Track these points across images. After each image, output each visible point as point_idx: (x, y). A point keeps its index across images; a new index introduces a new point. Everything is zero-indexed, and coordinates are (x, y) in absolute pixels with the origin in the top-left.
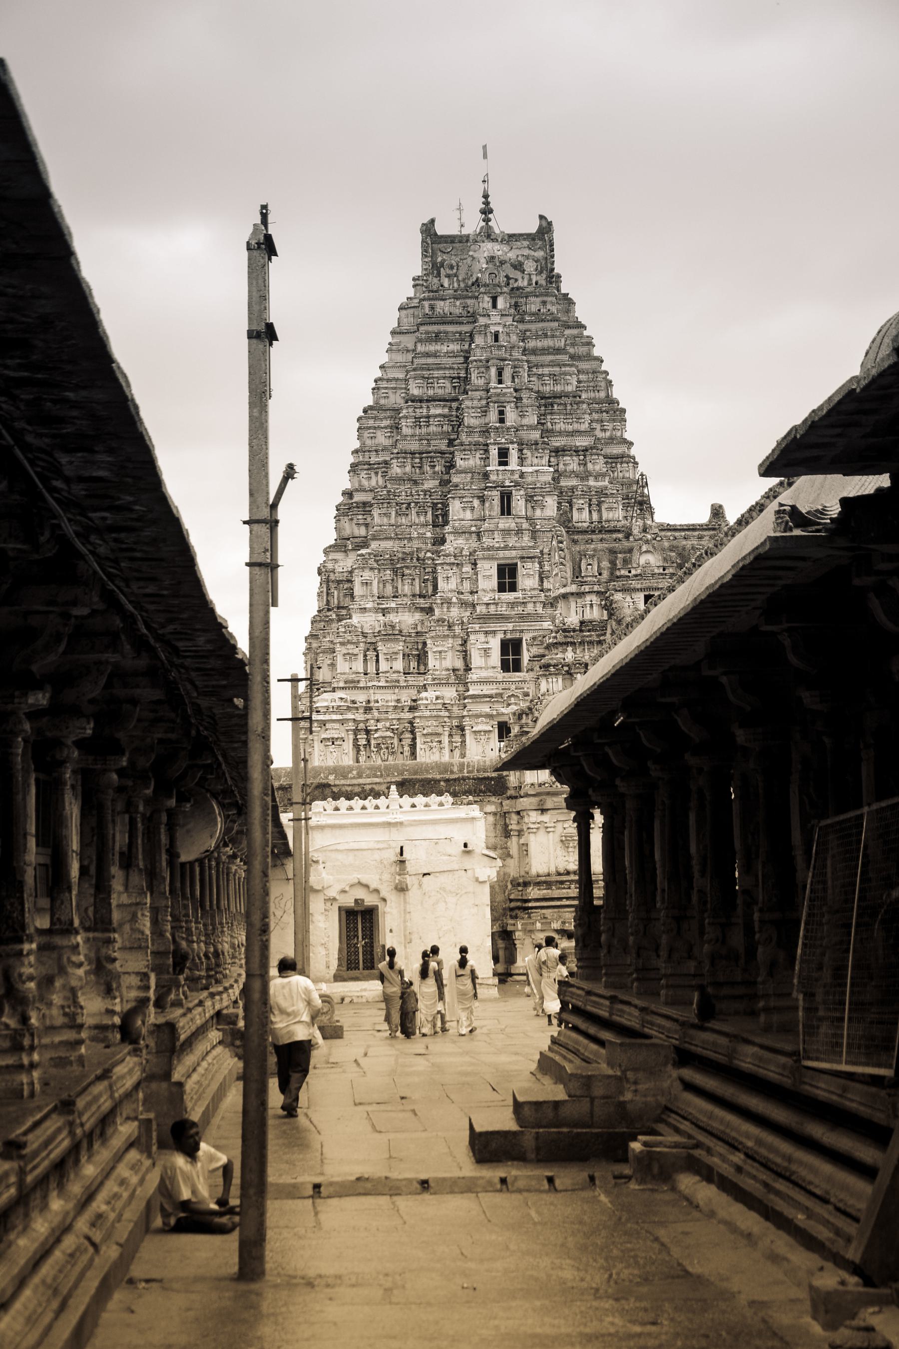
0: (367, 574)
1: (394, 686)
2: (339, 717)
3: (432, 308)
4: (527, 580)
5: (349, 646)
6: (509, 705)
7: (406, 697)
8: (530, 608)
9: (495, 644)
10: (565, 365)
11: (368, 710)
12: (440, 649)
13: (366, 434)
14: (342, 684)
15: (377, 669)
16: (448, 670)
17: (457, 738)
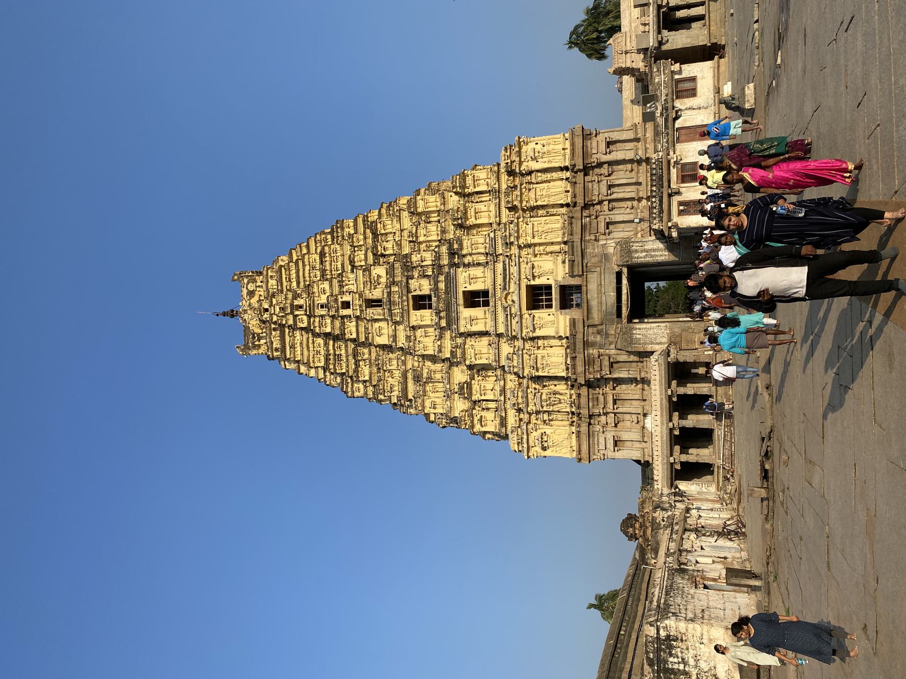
0: (428, 404)
2: (525, 437)
3: (277, 350)
5: (476, 421)
6: (513, 301)
7: (511, 382)
8: (442, 286)
9: (466, 313)
10: (303, 262)
11: (519, 410)
12: (473, 355)
13: (357, 394)
14: (503, 430)
15: (493, 401)
16: (489, 349)
17: (540, 342)
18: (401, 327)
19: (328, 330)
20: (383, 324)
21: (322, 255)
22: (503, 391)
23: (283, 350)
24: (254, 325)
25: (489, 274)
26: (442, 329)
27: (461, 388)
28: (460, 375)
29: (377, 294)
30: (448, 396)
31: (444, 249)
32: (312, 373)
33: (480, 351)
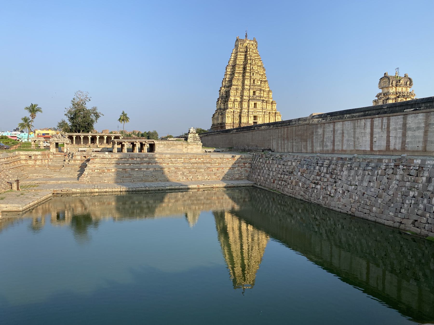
0: (232, 91)
1: (237, 109)
4: (257, 94)
8: (258, 98)
9: (253, 103)
18: (248, 87)
19: (247, 68)
20: (249, 83)
21: (260, 66)
22: (237, 109)
23: (240, 52)
24: (245, 44)
25: (260, 108)
26: (249, 97)
27: (237, 100)
28: (239, 99)
29: (256, 82)
30: (235, 96)
31: (263, 99)
32: (232, 57)
33: (245, 105)
